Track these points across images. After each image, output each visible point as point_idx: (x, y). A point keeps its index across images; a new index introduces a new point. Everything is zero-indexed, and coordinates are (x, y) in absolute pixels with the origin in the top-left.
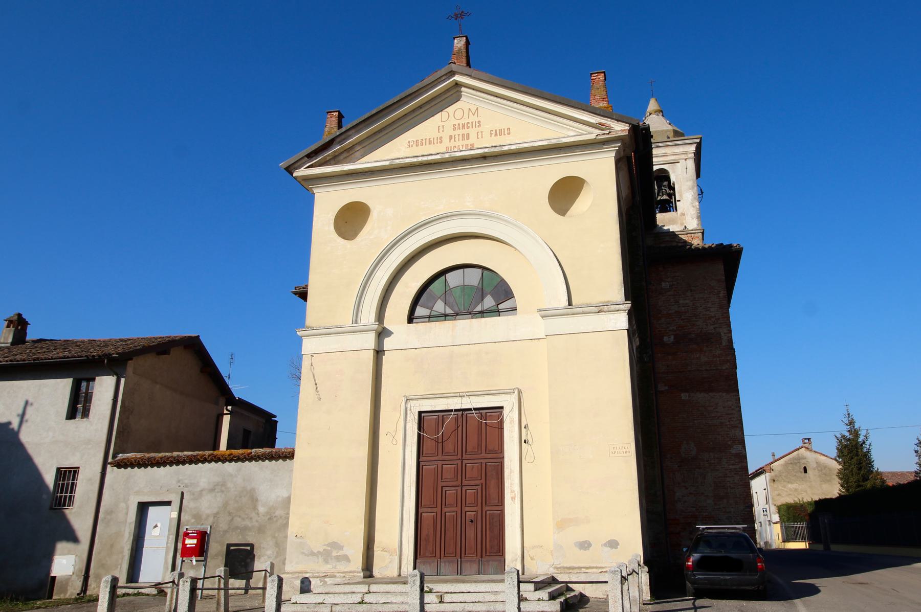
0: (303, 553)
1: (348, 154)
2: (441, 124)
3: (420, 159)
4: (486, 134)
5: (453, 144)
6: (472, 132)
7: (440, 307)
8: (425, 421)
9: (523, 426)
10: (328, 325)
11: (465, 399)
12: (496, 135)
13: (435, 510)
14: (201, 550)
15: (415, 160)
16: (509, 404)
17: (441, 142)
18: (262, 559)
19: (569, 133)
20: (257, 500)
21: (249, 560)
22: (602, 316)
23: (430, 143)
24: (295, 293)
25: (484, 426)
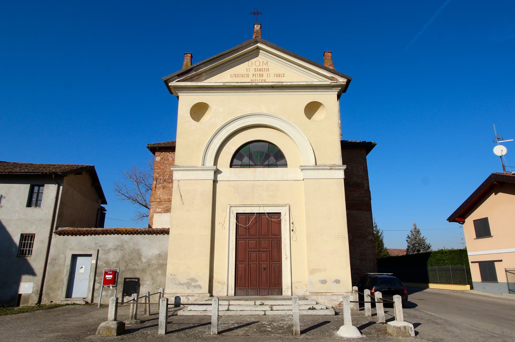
0: (175, 284)
1: (198, 77)
2: (248, 68)
3: (240, 84)
4: (272, 76)
5: (254, 78)
6: (265, 73)
7: (246, 160)
9: (291, 223)
10: (188, 166)
11: (261, 208)
12: (277, 76)
13: (244, 263)
14: (114, 282)
15: (237, 84)
16: (284, 212)
17: (248, 77)
18: (144, 286)
19: (316, 80)
20: (141, 255)
21: (137, 287)
22: (332, 171)
23: (242, 76)
24: (148, 148)
25: (270, 222)
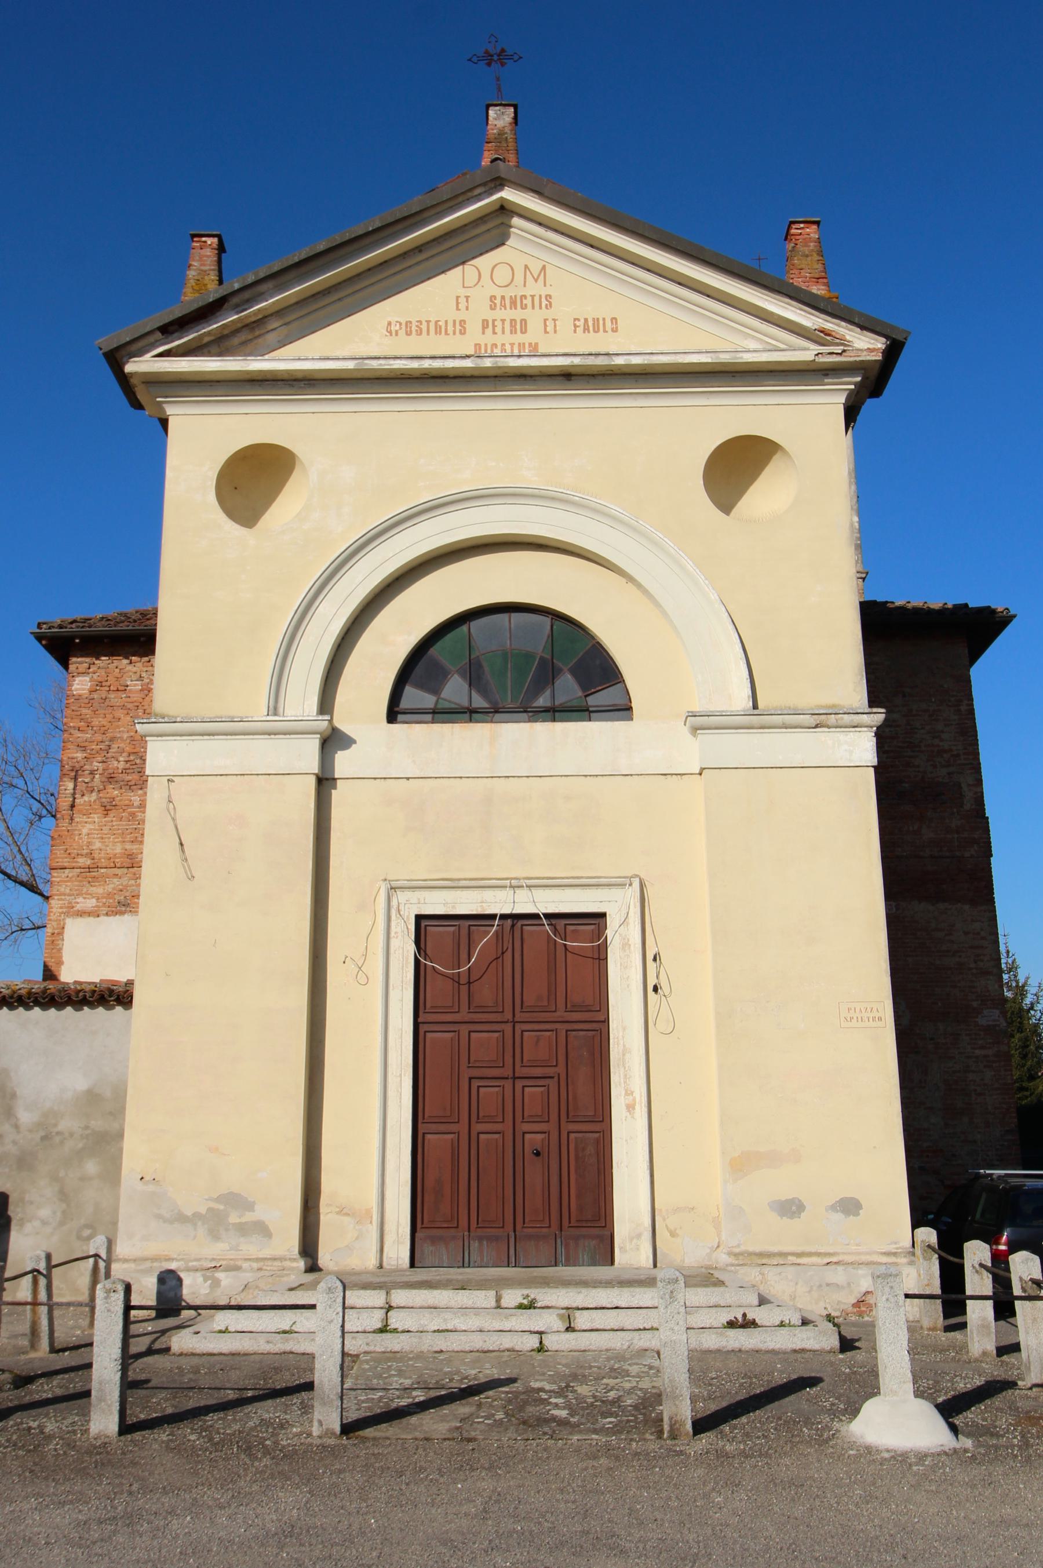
1: (248, 336)
2: (462, 292)
3: (426, 364)
4: (565, 326)
5: (488, 338)
6: (535, 318)
7: (456, 690)
8: (437, 937)
10: (209, 714)
11: (522, 895)
12: (586, 329)
13: (453, 1127)
15: (415, 365)
17: (463, 332)
18: (29, 1227)
20: (14, 1096)
22: (822, 735)
23: (438, 330)
24: (39, 638)
25: (560, 952)
